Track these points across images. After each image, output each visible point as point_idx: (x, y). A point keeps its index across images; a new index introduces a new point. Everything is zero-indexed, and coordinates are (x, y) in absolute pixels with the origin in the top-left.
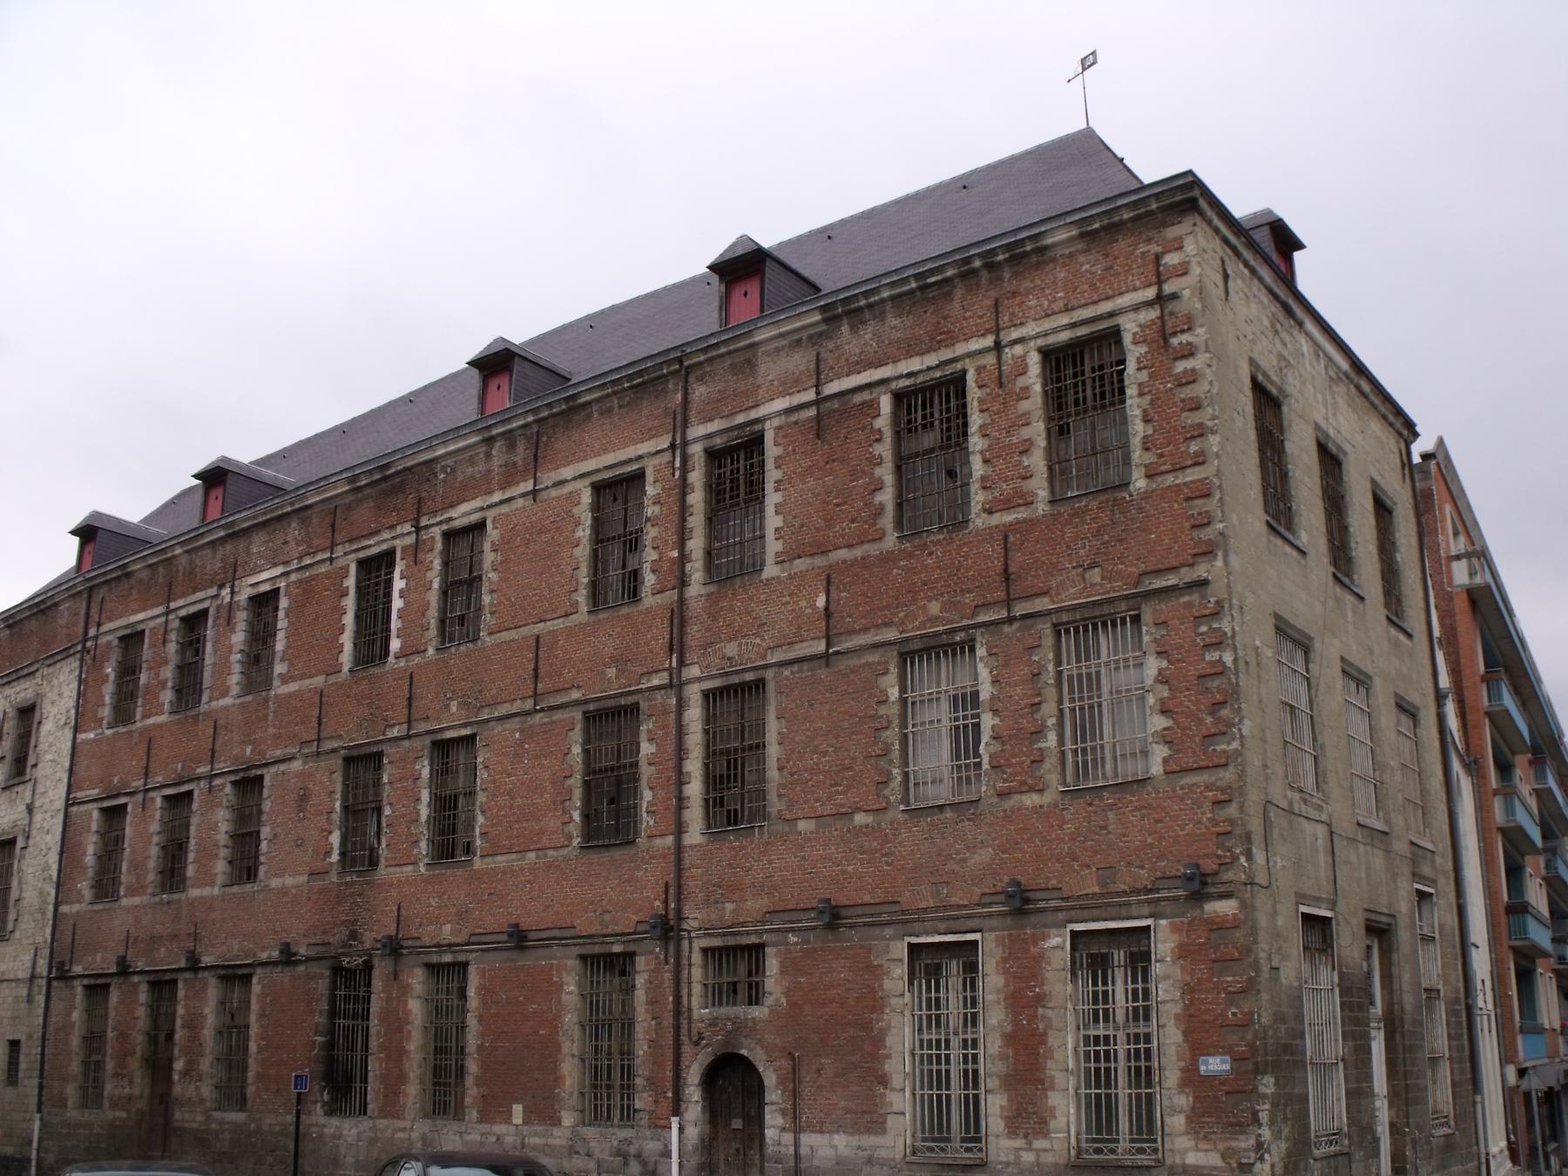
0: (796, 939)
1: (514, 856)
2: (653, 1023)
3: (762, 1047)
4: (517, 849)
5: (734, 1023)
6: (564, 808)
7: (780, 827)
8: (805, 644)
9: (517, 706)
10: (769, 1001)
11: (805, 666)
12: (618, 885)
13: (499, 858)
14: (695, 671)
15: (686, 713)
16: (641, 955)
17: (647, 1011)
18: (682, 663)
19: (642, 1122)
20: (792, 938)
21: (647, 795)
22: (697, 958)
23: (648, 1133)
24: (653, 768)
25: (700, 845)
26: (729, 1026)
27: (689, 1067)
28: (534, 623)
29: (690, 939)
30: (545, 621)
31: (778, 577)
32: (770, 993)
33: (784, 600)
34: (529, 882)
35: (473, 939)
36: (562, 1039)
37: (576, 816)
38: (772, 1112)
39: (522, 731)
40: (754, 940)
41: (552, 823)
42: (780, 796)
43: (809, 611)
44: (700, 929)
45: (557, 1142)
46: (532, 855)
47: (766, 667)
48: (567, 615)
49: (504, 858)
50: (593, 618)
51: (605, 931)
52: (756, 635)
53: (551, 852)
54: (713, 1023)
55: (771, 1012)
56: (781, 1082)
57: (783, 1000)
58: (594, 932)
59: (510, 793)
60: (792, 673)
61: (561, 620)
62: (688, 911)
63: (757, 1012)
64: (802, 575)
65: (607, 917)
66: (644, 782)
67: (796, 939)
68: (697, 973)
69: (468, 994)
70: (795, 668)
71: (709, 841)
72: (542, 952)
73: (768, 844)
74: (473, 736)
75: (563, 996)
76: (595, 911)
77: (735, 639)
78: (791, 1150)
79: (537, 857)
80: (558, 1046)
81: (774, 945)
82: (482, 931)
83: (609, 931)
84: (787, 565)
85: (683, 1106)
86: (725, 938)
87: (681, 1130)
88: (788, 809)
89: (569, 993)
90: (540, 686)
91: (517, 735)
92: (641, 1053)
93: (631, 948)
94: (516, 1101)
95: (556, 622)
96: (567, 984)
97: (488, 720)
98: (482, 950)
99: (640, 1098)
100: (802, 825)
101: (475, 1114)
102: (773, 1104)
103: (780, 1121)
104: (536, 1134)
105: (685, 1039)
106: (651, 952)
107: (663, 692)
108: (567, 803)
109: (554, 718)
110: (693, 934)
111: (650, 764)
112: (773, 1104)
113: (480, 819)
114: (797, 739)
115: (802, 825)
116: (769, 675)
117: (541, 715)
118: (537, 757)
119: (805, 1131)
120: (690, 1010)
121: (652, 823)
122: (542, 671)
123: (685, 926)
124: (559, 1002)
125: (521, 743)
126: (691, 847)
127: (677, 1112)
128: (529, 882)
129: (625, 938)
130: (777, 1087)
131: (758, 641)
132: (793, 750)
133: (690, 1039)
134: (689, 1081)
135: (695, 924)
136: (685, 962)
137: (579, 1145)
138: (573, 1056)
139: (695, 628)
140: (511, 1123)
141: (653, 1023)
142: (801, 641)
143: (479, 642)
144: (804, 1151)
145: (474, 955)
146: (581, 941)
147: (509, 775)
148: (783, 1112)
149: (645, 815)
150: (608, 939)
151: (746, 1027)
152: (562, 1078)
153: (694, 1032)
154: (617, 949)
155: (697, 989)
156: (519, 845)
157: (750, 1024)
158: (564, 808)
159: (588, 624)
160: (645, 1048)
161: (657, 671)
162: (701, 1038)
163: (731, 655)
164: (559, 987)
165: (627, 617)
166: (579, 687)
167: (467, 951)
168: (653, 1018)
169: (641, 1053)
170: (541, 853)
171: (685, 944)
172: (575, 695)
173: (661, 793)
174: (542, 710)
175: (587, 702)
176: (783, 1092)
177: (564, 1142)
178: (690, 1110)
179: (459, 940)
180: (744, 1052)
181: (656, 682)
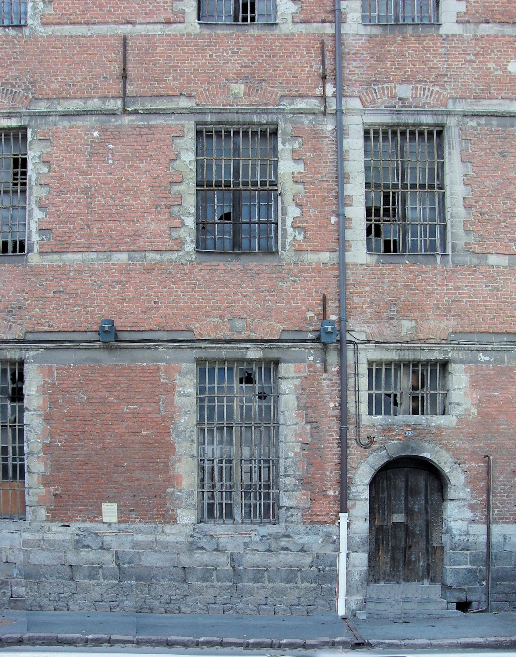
0: (487, 358)
1: (94, 256)
2: (308, 427)
3: (449, 450)
4: (100, 248)
5: (414, 429)
6: (171, 214)
7: (468, 259)
8: (494, 102)
9: (95, 104)
10: (456, 411)
11: (494, 121)
12: (254, 293)
13: (70, 256)
14: (355, 103)
15: (345, 141)
16: (285, 362)
17: (299, 415)
18: (339, 95)
19: (294, 519)
20: (483, 358)
21: (293, 211)
22: (363, 369)
23: (301, 528)
24: (301, 187)
25: (367, 265)
26: (409, 433)
27: (356, 468)
28: (115, 23)
29: (356, 351)
30: (133, 23)
31: (461, 36)
32: (458, 404)
33: (468, 58)
34: (119, 283)
35: (30, 337)
36: (173, 438)
37: (190, 222)
38: (458, 507)
39: (103, 130)
40: (436, 356)
41: (153, 226)
42: (467, 232)
43: (498, 73)
44: (369, 342)
45: (172, 539)
46: (124, 257)
47: (449, 114)
48: (168, 23)
49: (79, 256)
50: (206, 31)
51: (236, 337)
52: (434, 83)
53: (151, 256)
54: (388, 428)
55: (459, 420)
56: (471, 481)
57: (474, 410)
58: (220, 336)
59: (86, 191)
60: (479, 124)
61: (159, 26)
62: (353, 323)
63: (440, 420)
64: (491, 39)
65: (239, 324)
66: (288, 198)
67: (487, 358)
68: (364, 381)
69: (25, 392)
70: (483, 121)
71: (378, 261)
72: (147, 353)
73: (453, 272)
74: (24, 129)
75: (176, 398)
76: (222, 317)
77: (408, 82)
78: (483, 539)
79: (130, 258)
80: (171, 448)
81: (462, 362)
82: (46, 328)
83: (243, 336)
84: (471, 27)
85: (349, 503)
86: (401, 353)
87: (349, 525)
88: (477, 243)
89: (185, 395)
90: (130, 88)
91: (96, 134)
92: (291, 454)
93: (274, 354)
94: (108, 500)
95: (150, 27)
96: (183, 386)
97: (47, 115)
98: (46, 349)
99: (289, 497)
100: (493, 260)
101: (42, 513)
102: (460, 500)
103: (469, 514)
104: (139, 531)
105: (352, 443)
106: (303, 361)
107: (311, 117)
108: (176, 209)
109: (152, 123)
110: (360, 346)
111: (296, 182)
112: (460, 500)
113: (38, 214)
114: (487, 183)
115: (493, 260)
116: (451, 122)
117: (133, 117)
118: (126, 159)
119: (497, 522)
120: (358, 415)
121: (300, 237)
122: (132, 72)
123: (349, 338)
124: (171, 403)
125: (102, 143)
126: (355, 264)
127: (344, 509)
128: (119, 283)
129: (267, 345)
130: (466, 484)
131: (437, 89)
132: (482, 194)
133: (360, 444)
134: (357, 480)
135: (363, 337)
136: (350, 371)
137: (203, 542)
138: (193, 457)
139: (355, 64)
140: (101, 522)
141: (308, 427)
142: (490, 98)
143: (27, 31)
144: (494, 539)
145: (32, 353)
146: (203, 345)
147: (84, 173)
148: (472, 507)
149: (290, 230)
150: (243, 345)
151: (430, 432)
152: (179, 477)
153: (363, 435)
154: (253, 354)
155: (364, 397)
156: (103, 245)
157: (434, 431)
158: (171, 214)
159: (201, 36)
160: (297, 450)
161: (302, 96)
162: (372, 440)
163: (403, 96)
164: (170, 390)
165: (258, 38)
166: (190, 96)
167: (21, 349)
168: (307, 422)
169: (291, 454)
170: (137, 255)
171: (350, 355)
172: (184, 103)
173: (313, 212)
174: (135, 112)
175: (203, 113)
176: (473, 490)
177: (181, 539)
178: (357, 506)
179: (9, 337)
180: (426, 455)
181: (301, 104)
